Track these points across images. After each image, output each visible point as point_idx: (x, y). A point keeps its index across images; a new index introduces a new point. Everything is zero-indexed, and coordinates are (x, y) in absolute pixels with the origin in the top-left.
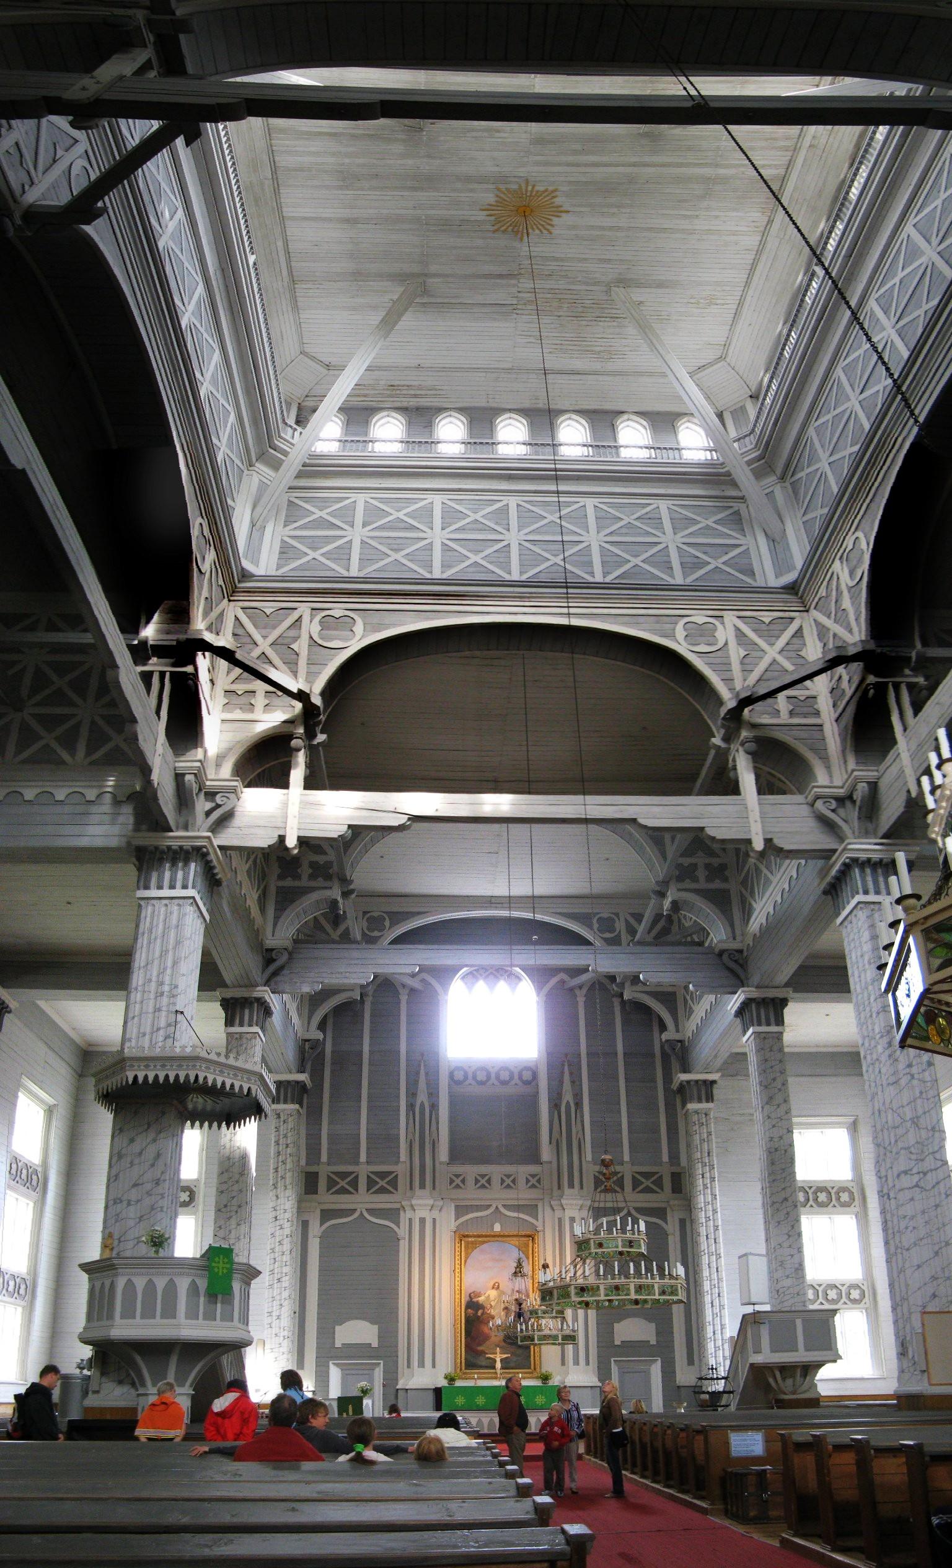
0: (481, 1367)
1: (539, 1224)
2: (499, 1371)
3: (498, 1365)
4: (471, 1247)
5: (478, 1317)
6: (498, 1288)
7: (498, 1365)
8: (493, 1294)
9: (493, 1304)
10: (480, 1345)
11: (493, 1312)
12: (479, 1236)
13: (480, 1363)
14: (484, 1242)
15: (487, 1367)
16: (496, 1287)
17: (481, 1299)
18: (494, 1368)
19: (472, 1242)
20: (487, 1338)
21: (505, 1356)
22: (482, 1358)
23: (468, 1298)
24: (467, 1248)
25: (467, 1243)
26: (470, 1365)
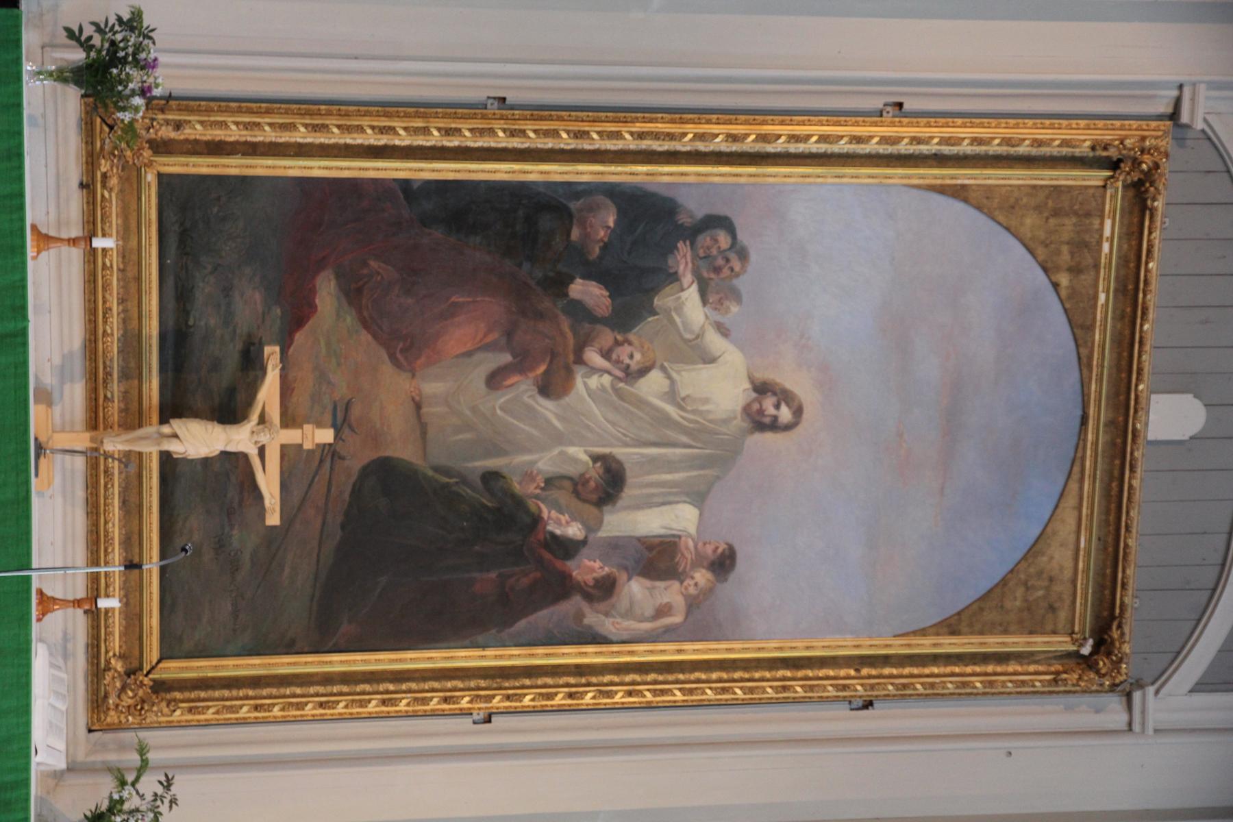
0: (179, 294)
1: (1173, 701)
2: (149, 443)
3: (199, 440)
4: (1054, 237)
5: (558, 285)
6: (761, 423)
7: (199, 440)
8: (722, 388)
9: (652, 385)
10: (352, 292)
11: (591, 383)
12: (1131, 290)
13: (205, 288)
14: (1080, 326)
15: (177, 342)
16: (769, 407)
17: (687, 305)
18: (172, 409)
19: (1085, 245)
20: (407, 347)
21: (269, 483)
22: (251, 304)
23: (695, 207)
24: (1056, 203)
25: (1084, 209)
26: (191, 215)
